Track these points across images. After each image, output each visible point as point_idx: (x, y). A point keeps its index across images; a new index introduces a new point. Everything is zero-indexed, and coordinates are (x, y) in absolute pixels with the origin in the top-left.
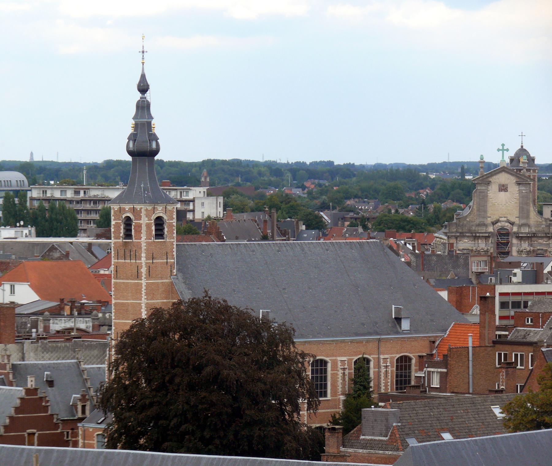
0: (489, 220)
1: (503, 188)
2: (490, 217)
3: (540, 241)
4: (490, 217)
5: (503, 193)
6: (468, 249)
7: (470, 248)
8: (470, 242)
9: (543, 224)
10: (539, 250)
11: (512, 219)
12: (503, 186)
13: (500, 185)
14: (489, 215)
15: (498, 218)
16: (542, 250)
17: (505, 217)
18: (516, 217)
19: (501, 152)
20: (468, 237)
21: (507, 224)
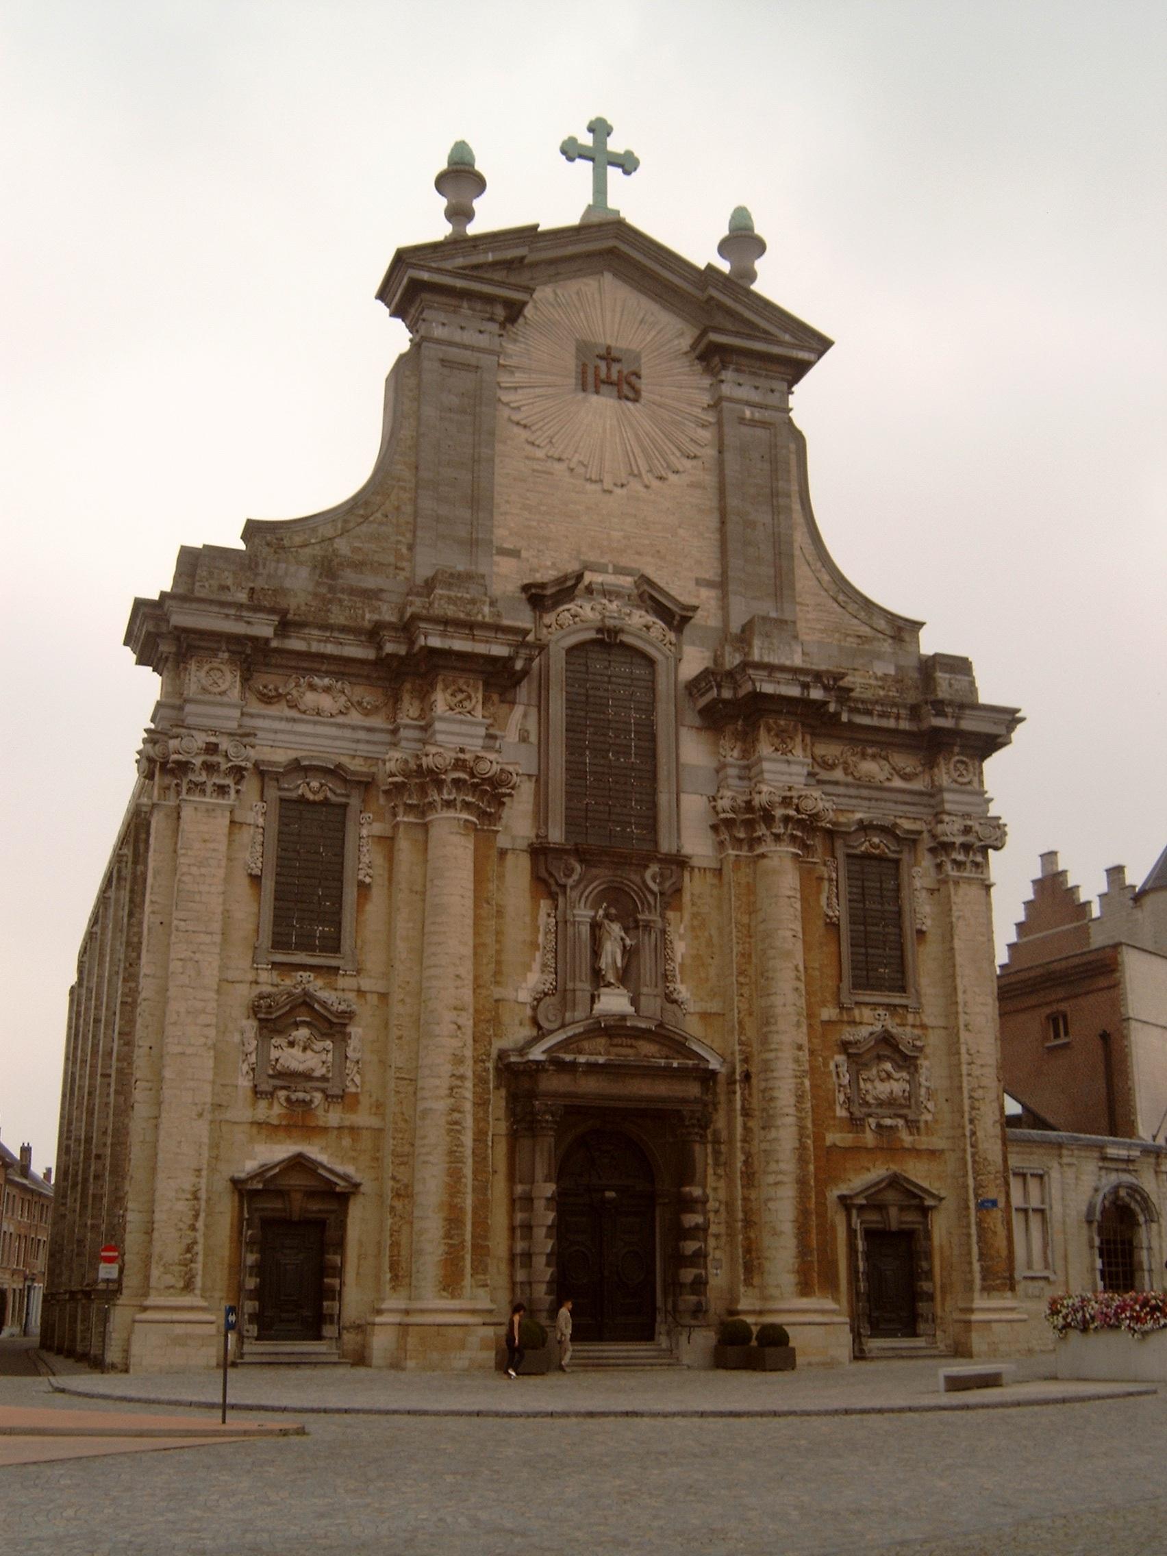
0: (506, 578)
1: (609, 373)
2: (515, 553)
3: (869, 767)
4: (515, 553)
5: (603, 404)
6: (336, 772)
7: (355, 765)
8: (355, 717)
9: (879, 656)
10: (865, 828)
11: (680, 587)
12: (609, 357)
13: (583, 348)
14: (502, 535)
15: (572, 567)
16: (888, 831)
17: (620, 571)
18: (699, 582)
19: (584, 168)
20: (342, 668)
21: (639, 618)
